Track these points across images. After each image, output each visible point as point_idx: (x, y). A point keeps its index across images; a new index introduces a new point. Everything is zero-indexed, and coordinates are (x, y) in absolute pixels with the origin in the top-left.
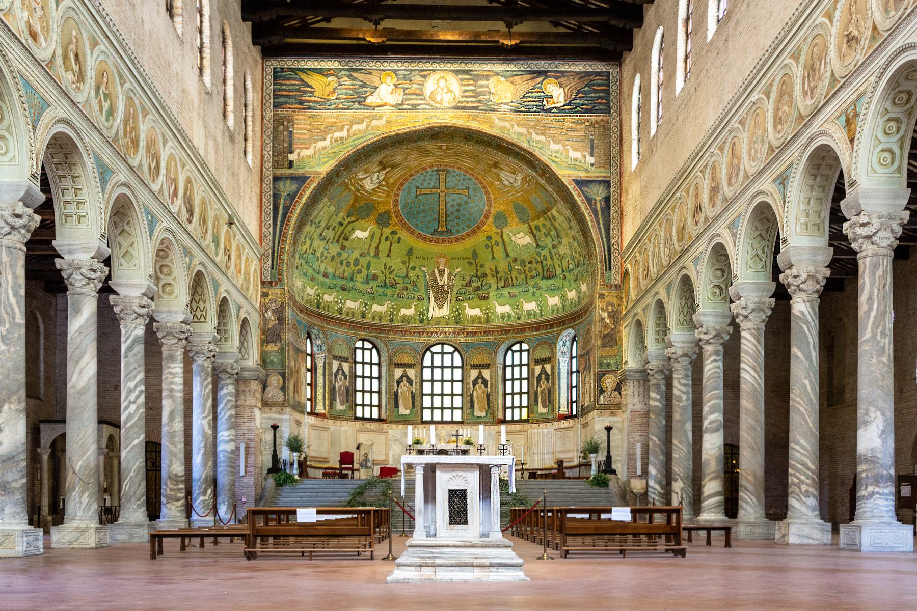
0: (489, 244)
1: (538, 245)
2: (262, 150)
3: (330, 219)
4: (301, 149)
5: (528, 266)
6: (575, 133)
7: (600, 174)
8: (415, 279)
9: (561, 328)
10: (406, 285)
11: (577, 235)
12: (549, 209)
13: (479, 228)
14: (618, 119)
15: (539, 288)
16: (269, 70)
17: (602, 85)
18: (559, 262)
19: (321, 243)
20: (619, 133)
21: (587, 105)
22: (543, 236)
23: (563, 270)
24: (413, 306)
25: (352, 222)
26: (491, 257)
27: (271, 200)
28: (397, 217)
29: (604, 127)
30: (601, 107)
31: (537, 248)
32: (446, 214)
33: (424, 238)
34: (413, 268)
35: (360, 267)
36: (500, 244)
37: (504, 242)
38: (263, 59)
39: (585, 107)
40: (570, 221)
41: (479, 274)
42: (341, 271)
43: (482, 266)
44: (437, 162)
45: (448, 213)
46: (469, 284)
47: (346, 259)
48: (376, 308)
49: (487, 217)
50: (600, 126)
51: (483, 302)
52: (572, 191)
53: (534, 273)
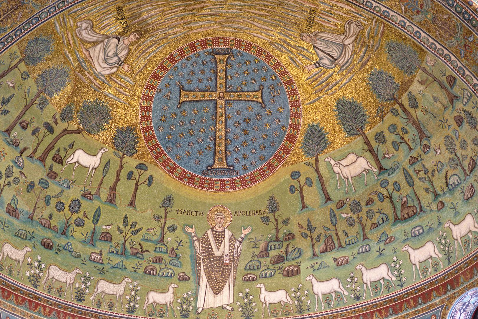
0: (297, 186)
1: (381, 168)
3: (27, 107)
5: (365, 209)
8: (175, 245)
9: (449, 294)
10: (159, 254)
11: (469, 108)
12: (407, 84)
13: (280, 159)
15: (389, 240)
18: (428, 185)
19: (7, 149)
22: (392, 149)
23: (436, 195)
24: (171, 290)
25: (71, 132)
26: (300, 206)
28: (147, 140)
31: (380, 174)
32: (226, 139)
33: (191, 181)
34: (173, 229)
35: (81, 215)
36: (315, 182)
37: (321, 179)
40: (452, 81)
41: (281, 236)
42: (46, 215)
43: (286, 222)
45: (230, 136)
46: (265, 252)
47: (56, 196)
48: (104, 287)
49: (291, 139)
51: (291, 280)
53: (377, 218)
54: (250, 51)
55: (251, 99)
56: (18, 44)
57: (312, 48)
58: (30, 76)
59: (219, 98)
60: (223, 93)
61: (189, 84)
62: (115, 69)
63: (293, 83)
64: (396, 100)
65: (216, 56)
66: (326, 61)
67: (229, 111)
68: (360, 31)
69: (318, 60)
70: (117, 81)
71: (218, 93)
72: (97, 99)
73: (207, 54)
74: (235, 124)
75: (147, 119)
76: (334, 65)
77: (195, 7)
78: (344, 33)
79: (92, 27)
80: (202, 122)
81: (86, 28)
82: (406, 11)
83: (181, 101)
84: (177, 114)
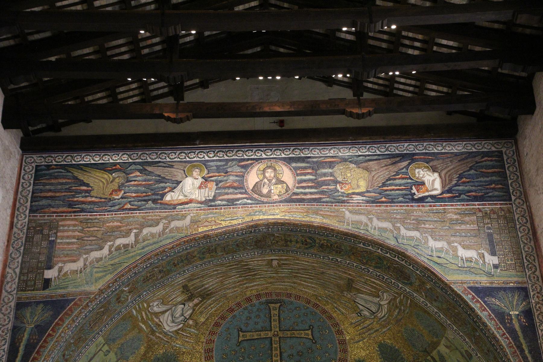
2: (5, 266)
4: (65, 262)
6: (463, 227)
7: (510, 279)
14: (525, 207)
16: (30, 169)
17: (493, 167)
20: (529, 225)
21: (475, 191)
27: (8, 337)
29: (505, 218)
30: (496, 193)
38: (23, 155)
39: (474, 194)
44: (267, 289)
50: (499, 217)
52: (471, 303)
54: (299, 300)
55: (303, 336)
56: (103, 336)
57: (353, 302)
58: (111, 352)
59: (273, 336)
60: (277, 332)
61: (247, 327)
62: (182, 325)
63: (339, 325)
64: (428, 353)
65: (270, 305)
66: (366, 313)
67: (283, 346)
68: (391, 299)
69: (359, 310)
70: (183, 333)
71: (273, 332)
72: (166, 351)
73: (261, 303)
74: (289, 356)
75: (210, 358)
76: (373, 317)
77: (249, 274)
78: (378, 296)
79: (163, 303)
80: (259, 356)
81: (157, 305)
82: (426, 296)
83: (240, 340)
84: (237, 351)
